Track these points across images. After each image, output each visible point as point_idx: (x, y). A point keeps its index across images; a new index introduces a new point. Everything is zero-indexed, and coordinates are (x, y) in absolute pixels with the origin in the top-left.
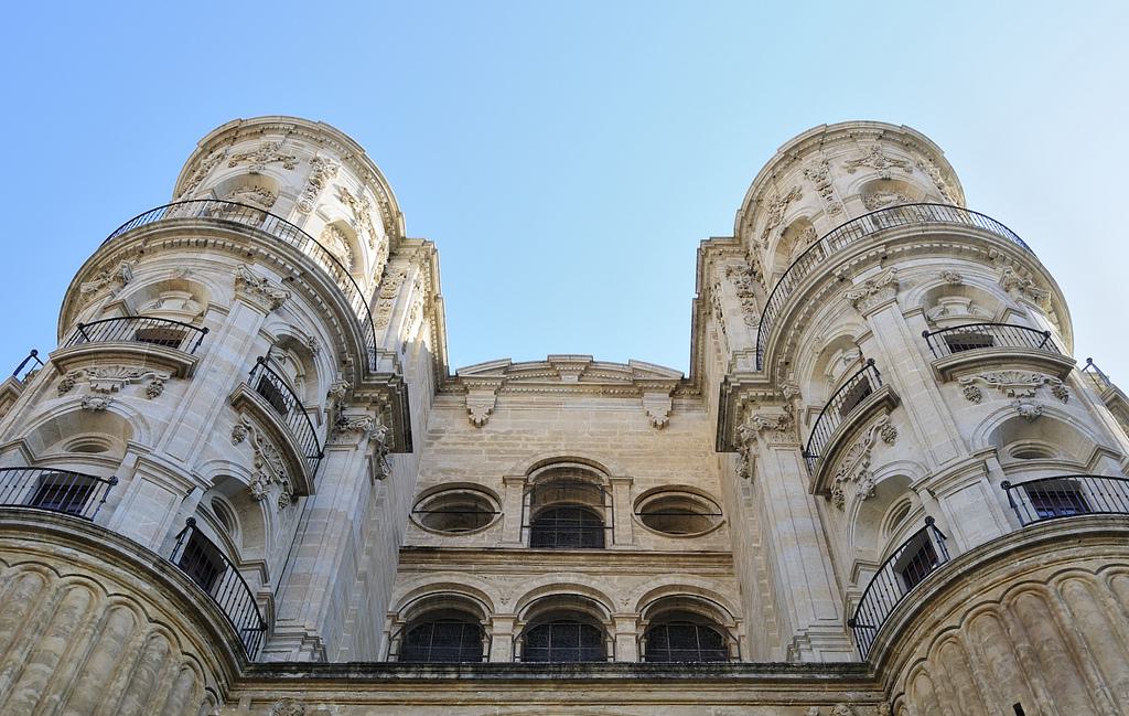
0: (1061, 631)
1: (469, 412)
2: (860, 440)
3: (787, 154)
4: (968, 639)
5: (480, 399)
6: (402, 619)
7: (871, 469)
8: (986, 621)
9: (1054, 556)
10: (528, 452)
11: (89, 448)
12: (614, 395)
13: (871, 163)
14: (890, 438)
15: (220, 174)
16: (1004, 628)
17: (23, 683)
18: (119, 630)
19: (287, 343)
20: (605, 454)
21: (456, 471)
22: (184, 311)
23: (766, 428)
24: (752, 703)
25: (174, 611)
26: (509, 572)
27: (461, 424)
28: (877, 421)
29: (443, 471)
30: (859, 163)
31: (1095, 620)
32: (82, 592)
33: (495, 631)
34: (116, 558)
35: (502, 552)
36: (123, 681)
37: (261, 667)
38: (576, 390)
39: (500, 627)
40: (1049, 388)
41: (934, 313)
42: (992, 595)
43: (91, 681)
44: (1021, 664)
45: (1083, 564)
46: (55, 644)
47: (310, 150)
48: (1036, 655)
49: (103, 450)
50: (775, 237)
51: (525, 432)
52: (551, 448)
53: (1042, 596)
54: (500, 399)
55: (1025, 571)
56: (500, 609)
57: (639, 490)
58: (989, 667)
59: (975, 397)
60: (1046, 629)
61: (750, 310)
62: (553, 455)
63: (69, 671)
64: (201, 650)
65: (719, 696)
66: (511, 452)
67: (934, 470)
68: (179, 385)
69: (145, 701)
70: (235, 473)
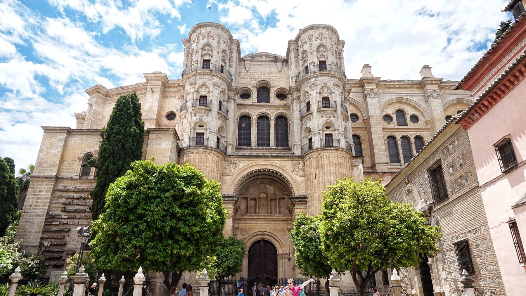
3: (306, 29)
4: (312, 160)
5: (247, 63)
8: (315, 159)
14: (310, 120)
15: (202, 42)
27: (244, 70)
28: (310, 116)
29: (242, 83)
30: (318, 38)
32: (209, 156)
35: (253, 105)
37: (228, 156)
38: (265, 61)
42: (316, 155)
43: (213, 168)
46: (208, 164)
47: (216, 31)
48: (318, 165)
49: (203, 126)
53: (321, 157)
59: (322, 117)
60: (320, 162)
65: (283, 159)
67: (314, 131)
68: (211, 112)
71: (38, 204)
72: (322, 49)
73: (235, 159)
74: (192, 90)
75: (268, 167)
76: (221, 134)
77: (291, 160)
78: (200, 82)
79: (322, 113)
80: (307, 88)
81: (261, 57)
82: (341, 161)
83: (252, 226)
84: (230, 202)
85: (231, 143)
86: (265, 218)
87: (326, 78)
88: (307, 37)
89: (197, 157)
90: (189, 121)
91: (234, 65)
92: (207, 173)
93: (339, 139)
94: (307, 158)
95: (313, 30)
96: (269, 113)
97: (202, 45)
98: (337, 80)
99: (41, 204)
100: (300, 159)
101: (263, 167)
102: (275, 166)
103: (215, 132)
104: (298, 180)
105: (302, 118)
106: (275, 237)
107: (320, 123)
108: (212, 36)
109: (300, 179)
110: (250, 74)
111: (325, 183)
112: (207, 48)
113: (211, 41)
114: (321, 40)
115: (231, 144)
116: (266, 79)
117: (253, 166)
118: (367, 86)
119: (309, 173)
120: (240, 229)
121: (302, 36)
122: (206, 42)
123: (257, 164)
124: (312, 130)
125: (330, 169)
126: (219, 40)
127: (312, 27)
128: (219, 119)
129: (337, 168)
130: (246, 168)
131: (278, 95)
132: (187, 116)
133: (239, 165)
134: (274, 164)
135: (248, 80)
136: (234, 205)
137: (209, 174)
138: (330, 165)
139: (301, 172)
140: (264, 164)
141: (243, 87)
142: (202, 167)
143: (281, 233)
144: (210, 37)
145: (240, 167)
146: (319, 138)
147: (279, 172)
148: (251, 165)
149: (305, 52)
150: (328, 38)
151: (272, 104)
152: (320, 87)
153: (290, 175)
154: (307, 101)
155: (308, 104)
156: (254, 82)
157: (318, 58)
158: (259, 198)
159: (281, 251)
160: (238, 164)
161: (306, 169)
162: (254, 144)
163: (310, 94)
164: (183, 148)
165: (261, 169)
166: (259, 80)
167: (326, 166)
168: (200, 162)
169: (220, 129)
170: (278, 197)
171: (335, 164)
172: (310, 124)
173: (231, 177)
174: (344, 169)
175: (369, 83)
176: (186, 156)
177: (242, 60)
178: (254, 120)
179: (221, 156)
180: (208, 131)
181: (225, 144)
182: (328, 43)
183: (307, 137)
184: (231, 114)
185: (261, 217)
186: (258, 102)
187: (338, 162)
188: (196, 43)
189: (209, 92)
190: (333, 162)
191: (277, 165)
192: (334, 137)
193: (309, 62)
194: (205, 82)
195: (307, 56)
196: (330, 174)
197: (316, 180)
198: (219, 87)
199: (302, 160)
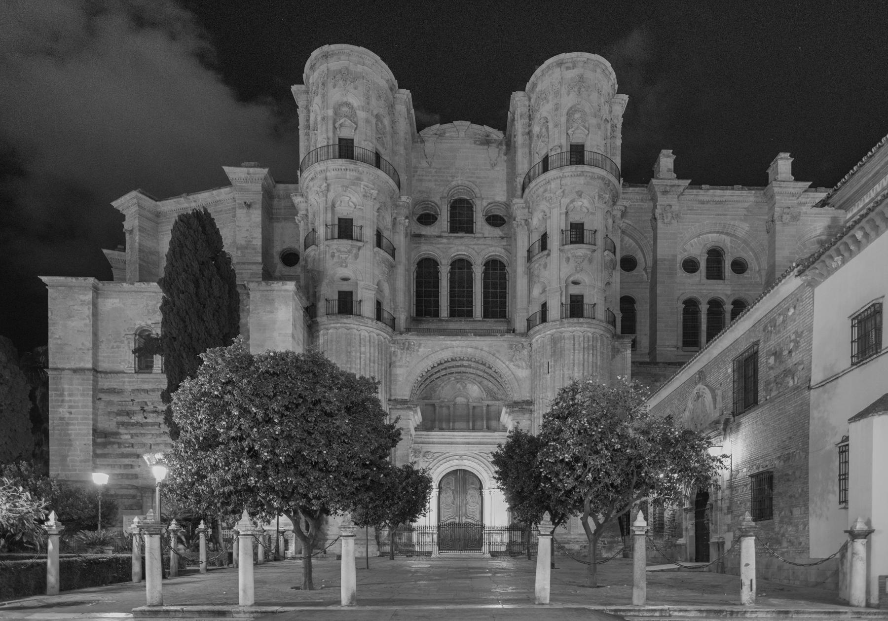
10: (448, 181)
20: (473, 182)
36: (377, 354)
43: (372, 355)
46: (363, 349)
48: (555, 351)
63: (368, 355)
71: (72, 416)
91: (402, 150)
92: (363, 362)
99: (80, 416)
104: (520, 375)
125: (574, 358)
129: (586, 356)
131: (489, 217)
133: (418, 351)
162: (444, 312)
167: (567, 352)
184: (401, 254)
196: (574, 366)
197: (549, 376)
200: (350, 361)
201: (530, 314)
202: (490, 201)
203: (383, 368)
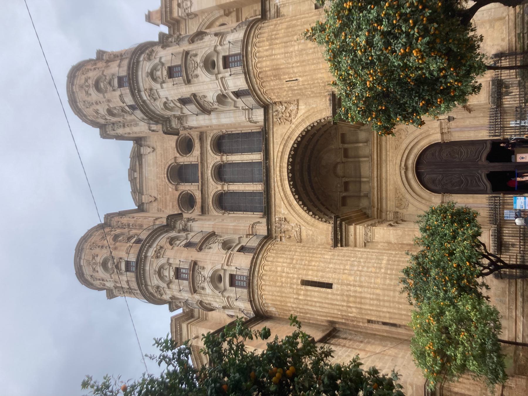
0: (270, 70)
1: (150, 202)
2: (202, 103)
3: (78, 112)
4: (268, 88)
6: (223, 211)
7: (212, 102)
9: (251, 68)
11: (220, 279)
12: (142, 162)
13: (87, 89)
14: (205, 97)
15: (101, 273)
16: (267, 81)
17: (289, 272)
18: (272, 259)
19: (171, 244)
21: (173, 204)
22: (168, 269)
23: (181, 124)
24: (273, 132)
25: (263, 251)
26: (208, 188)
27: (155, 204)
28: (198, 97)
29: (173, 207)
30: (87, 93)
31: (268, 63)
32: (265, 268)
33: (226, 189)
34: (256, 263)
38: (141, 173)
39: (226, 188)
40: (193, 58)
41: (160, 80)
43: (285, 260)
44: (276, 79)
45: (253, 63)
46: (279, 269)
48: (275, 76)
50: (108, 117)
51: (157, 186)
52: (164, 179)
53: (260, 72)
54: (145, 193)
55: (254, 75)
56: (220, 188)
57: (178, 155)
58: (275, 85)
59: (197, 76)
60: (269, 73)
61: (131, 125)
62: (166, 178)
63: (284, 264)
64: (269, 244)
65: (271, 139)
66: (165, 189)
68: (199, 263)
69: (285, 251)
70: (220, 246)
72: (102, 85)
73: (274, 220)
74: (168, 291)
75: (285, 165)
76: (234, 244)
77: (271, 126)
78: (155, 279)
79: (190, 78)
80: (158, 105)
81: (135, 178)
82: (266, 35)
83: (391, 187)
84: (344, 230)
85: (251, 226)
86: (376, 165)
87: (140, 73)
88: (88, 109)
89: (268, 288)
90: (212, 299)
92: (292, 271)
93: (229, 42)
94: (266, 99)
95: (78, 101)
96: (212, 164)
97: (106, 274)
98: (143, 56)
100: (271, 111)
101: (285, 174)
102: (282, 152)
103: (228, 255)
104: (303, 111)
105: (205, 110)
106: (410, 147)
107: (207, 80)
108: (94, 258)
109: (303, 108)
110: (160, 194)
111: (303, 61)
112: (110, 265)
113: (99, 259)
114: (88, 86)
115: (252, 227)
116: (166, 170)
117: (283, 190)
118: (175, 15)
119: (290, 92)
120: (397, 210)
121: (89, 117)
122: (101, 268)
123: (279, 184)
124: (220, 92)
125: (279, 54)
126: (99, 247)
127: (73, 102)
128: (210, 248)
129: (278, 41)
130: (288, 202)
132: (207, 302)
133: (284, 214)
134: (280, 154)
135: (168, 197)
136: (350, 224)
137: (294, 268)
138: (272, 55)
139: (292, 107)
140: (280, 171)
141: (177, 205)
142: (284, 280)
143: (403, 137)
144: (94, 261)
145: (286, 212)
146: (230, 78)
147: (293, 146)
148: (282, 194)
149: (110, 112)
150: (85, 76)
151: (199, 161)
152: (153, 83)
153: (297, 126)
154: (179, 105)
155: (184, 101)
156: (171, 188)
157: (114, 90)
158: (343, 177)
159: (436, 135)
160: (282, 216)
161: (285, 99)
163: (165, 100)
164: (254, 312)
165: (288, 177)
166: (167, 181)
167: (275, 62)
168: (276, 282)
169: (227, 246)
170: (341, 145)
171: (270, 45)
172: (211, 96)
173: (303, 228)
174: (280, 28)
175: (171, 12)
176: (268, 307)
177: (141, 208)
178: (223, 187)
179: (269, 246)
180: (225, 267)
181: (251, 237)
182: (93, 75)
183: (235, 101)
185: (375, 173)
186: (198, 182)
187: (267, 40)
188: (105, 283)
189: (170, 265)
190: (267, 50)
191: (281, 150)
192: (227, 54)
193: (122, 104)
194: (155, 271)
195: (115, 108)
196: (287, 53)
197: (300, 79)
198: (161, 248)
199: (271, 106)
200: (291, 284)
201: (247, 107)
202: (176, 151)
203: (298, 250)
